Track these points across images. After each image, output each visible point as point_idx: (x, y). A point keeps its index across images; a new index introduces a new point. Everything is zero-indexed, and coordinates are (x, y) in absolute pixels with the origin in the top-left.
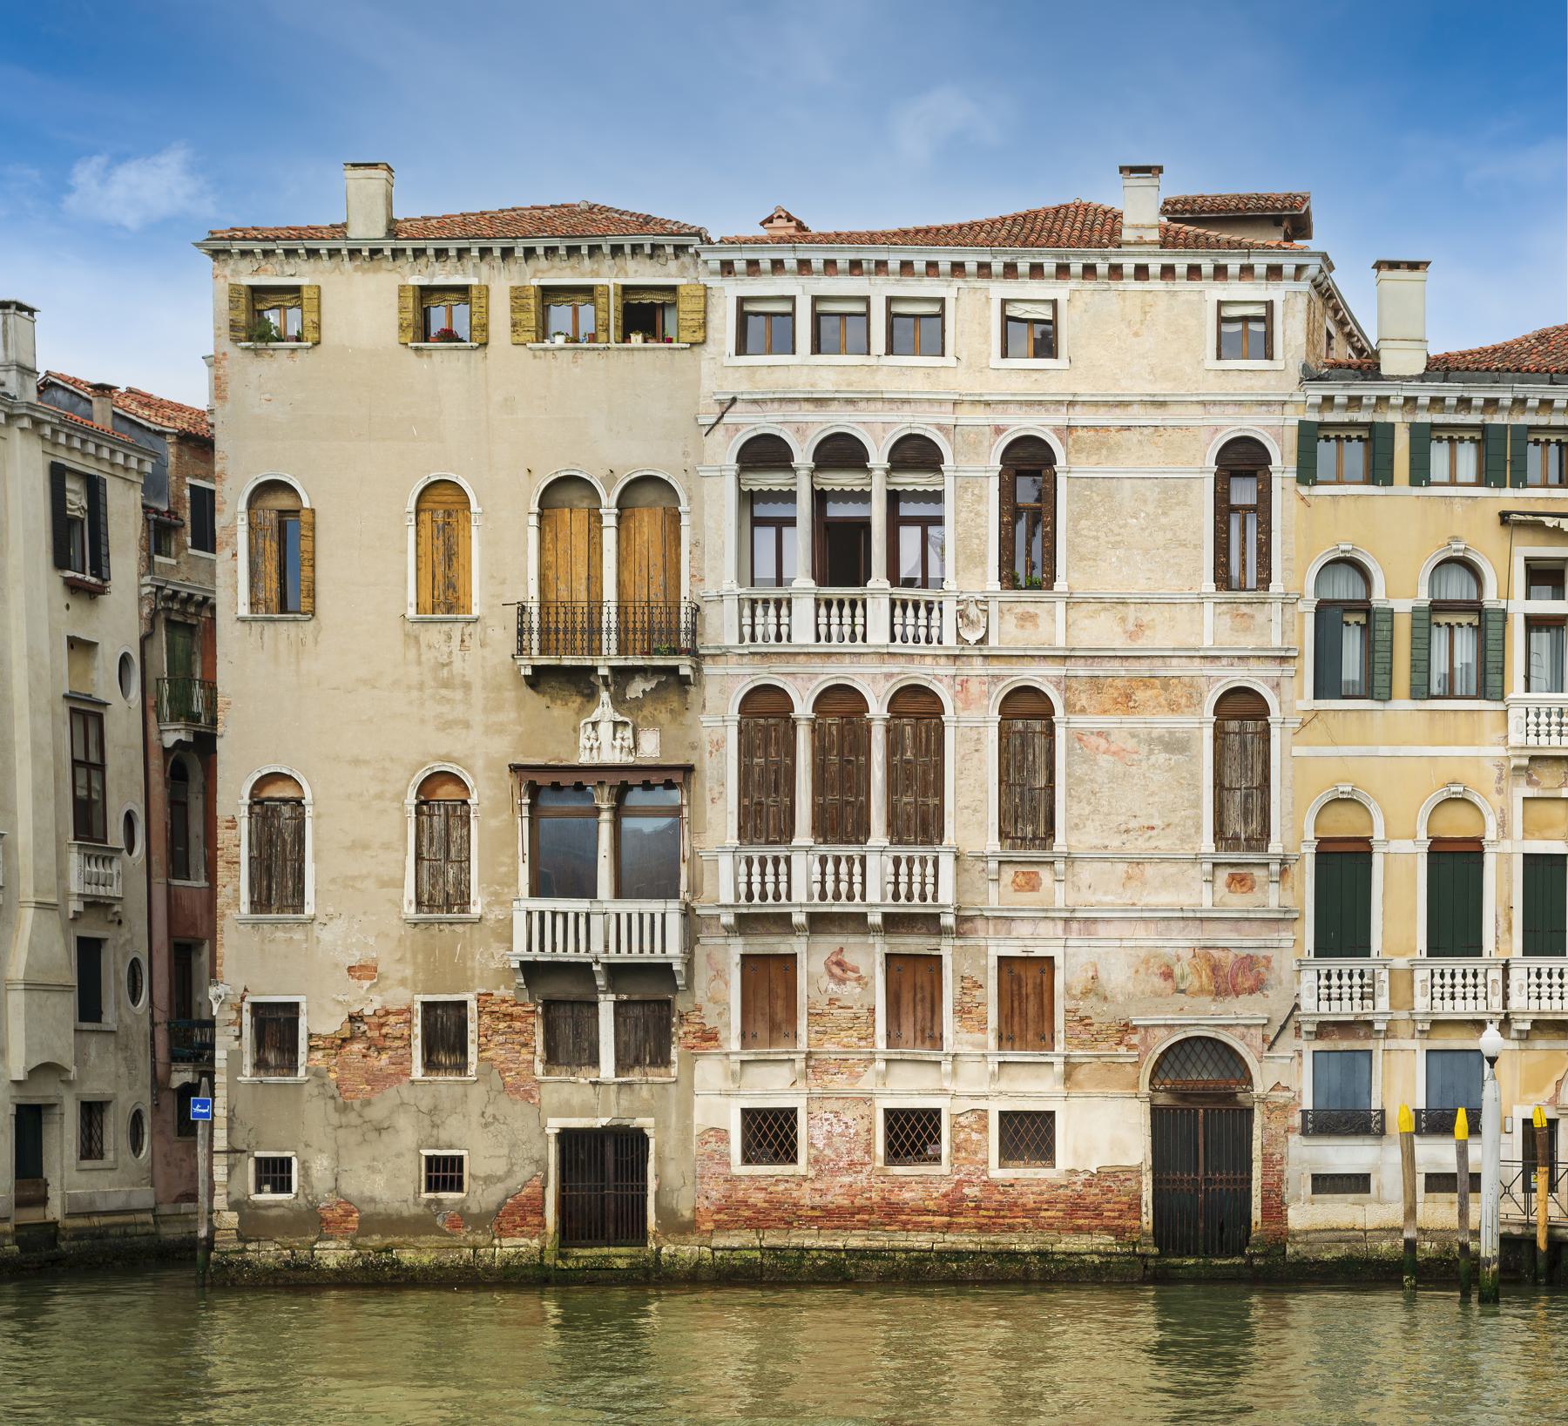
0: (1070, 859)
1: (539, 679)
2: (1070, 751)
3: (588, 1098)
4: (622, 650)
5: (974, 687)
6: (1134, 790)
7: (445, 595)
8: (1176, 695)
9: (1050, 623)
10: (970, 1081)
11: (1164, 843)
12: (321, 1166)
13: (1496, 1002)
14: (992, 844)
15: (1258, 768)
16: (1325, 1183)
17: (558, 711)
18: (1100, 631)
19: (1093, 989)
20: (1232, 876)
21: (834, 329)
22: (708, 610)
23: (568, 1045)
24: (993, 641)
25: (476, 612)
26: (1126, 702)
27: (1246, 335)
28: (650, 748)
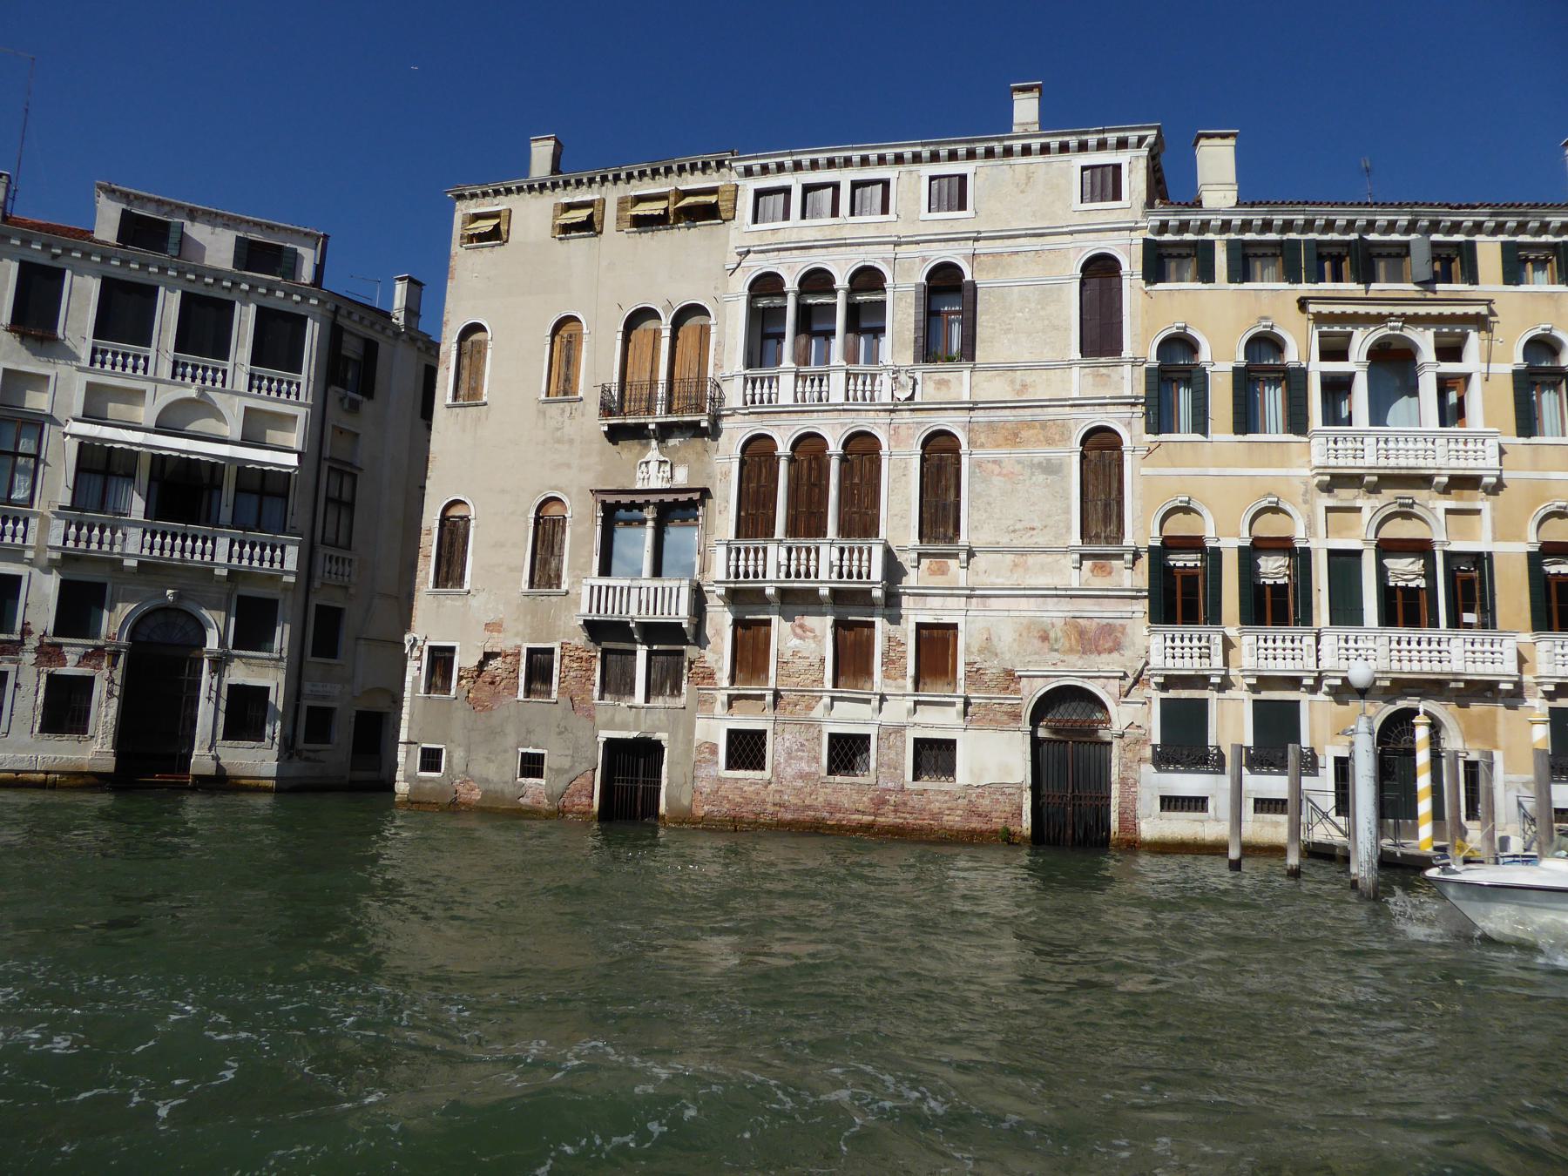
1: (615, 434)
3: (632, 715)
4: (669, 411)
5: (903, 431)
6: (1020, 502)
7: (563, 382)
8: (1051, 433)
9: (960, 383)
10: (892, 711)
11: (1041, 540)
12: (459, 754)
13: (1310, 663)
14: (913, 539)
15: (1115, 485)
16: (1170, 803)
17: (625, 455)
18: (994, 388)
19: (988, 648)
20: (1095, 566)
22: (724, 386)
23: (617, 683)
24: (917, 398)
25: (580, 394)
26: (1013, 437)
27: (1105, 184)
28: (681, 478)
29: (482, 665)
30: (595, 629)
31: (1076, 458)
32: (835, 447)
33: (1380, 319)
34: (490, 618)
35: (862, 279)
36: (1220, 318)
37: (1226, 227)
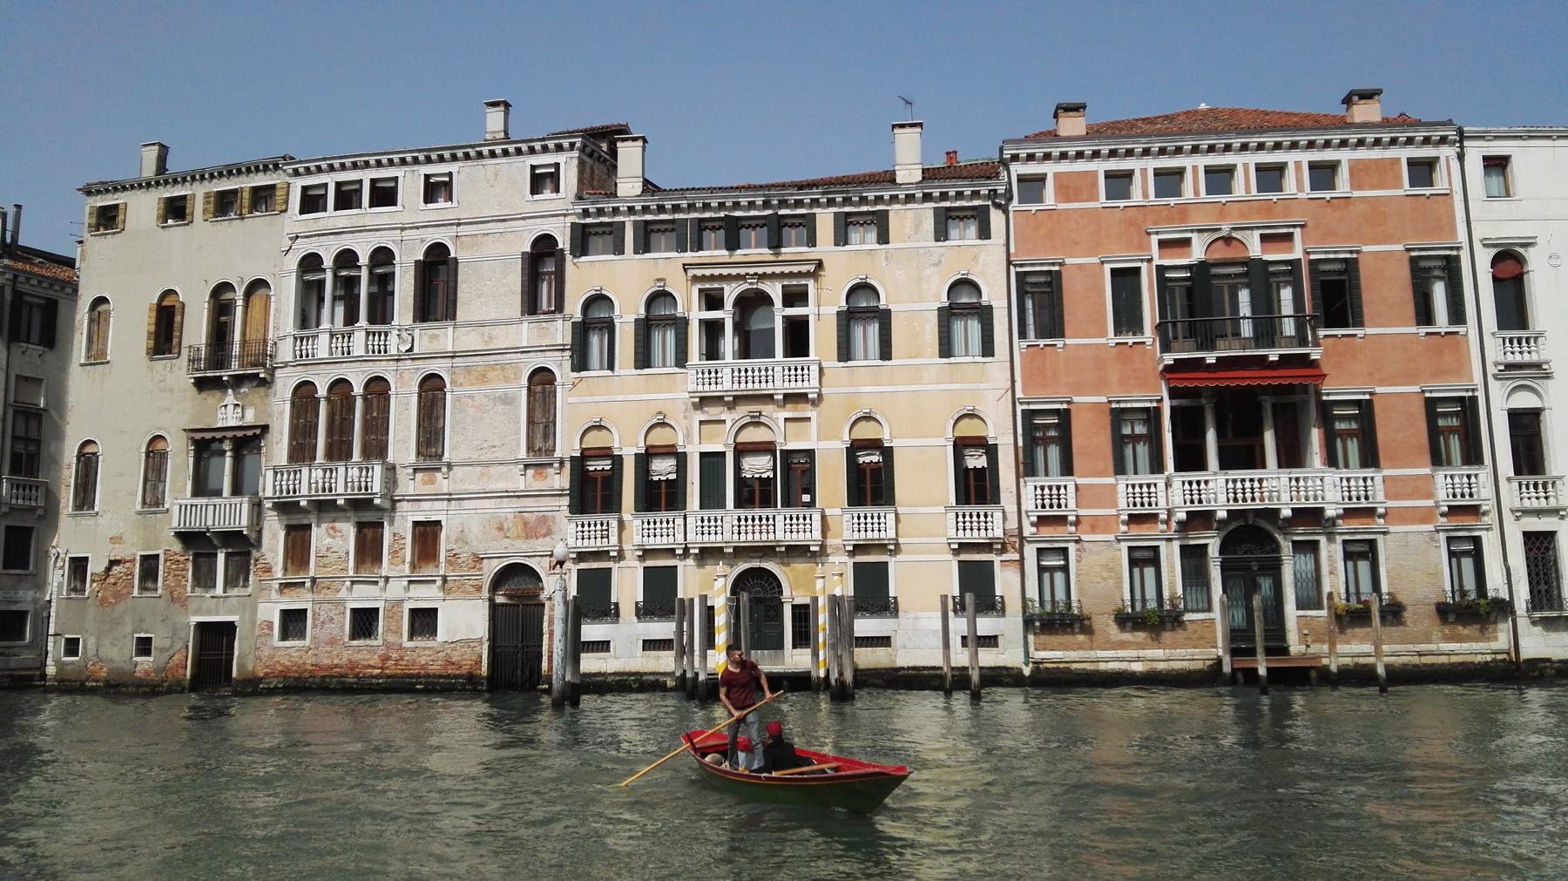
0: (450, 466)
1: (202, 384)
2: (454, 406)
3: (216, 605)
4: (242, 366)
5: (406, 374)
6: (485, 424)
9: (441, 337)
11: (500, 455)
12: (92, 642)
14: (412, 458)
19: (462, 539)
21: (347, 198)
22: (280, 344)
23: (204, 578)
28: (250, 418)
29: (108, 569)
30: (186, 538)
31: (525, 392)
32: (358, 389)
33: (739, 277)
34: (114, 532)
35: (381, 256)
36: (623, 278)
37: (631, 210)
